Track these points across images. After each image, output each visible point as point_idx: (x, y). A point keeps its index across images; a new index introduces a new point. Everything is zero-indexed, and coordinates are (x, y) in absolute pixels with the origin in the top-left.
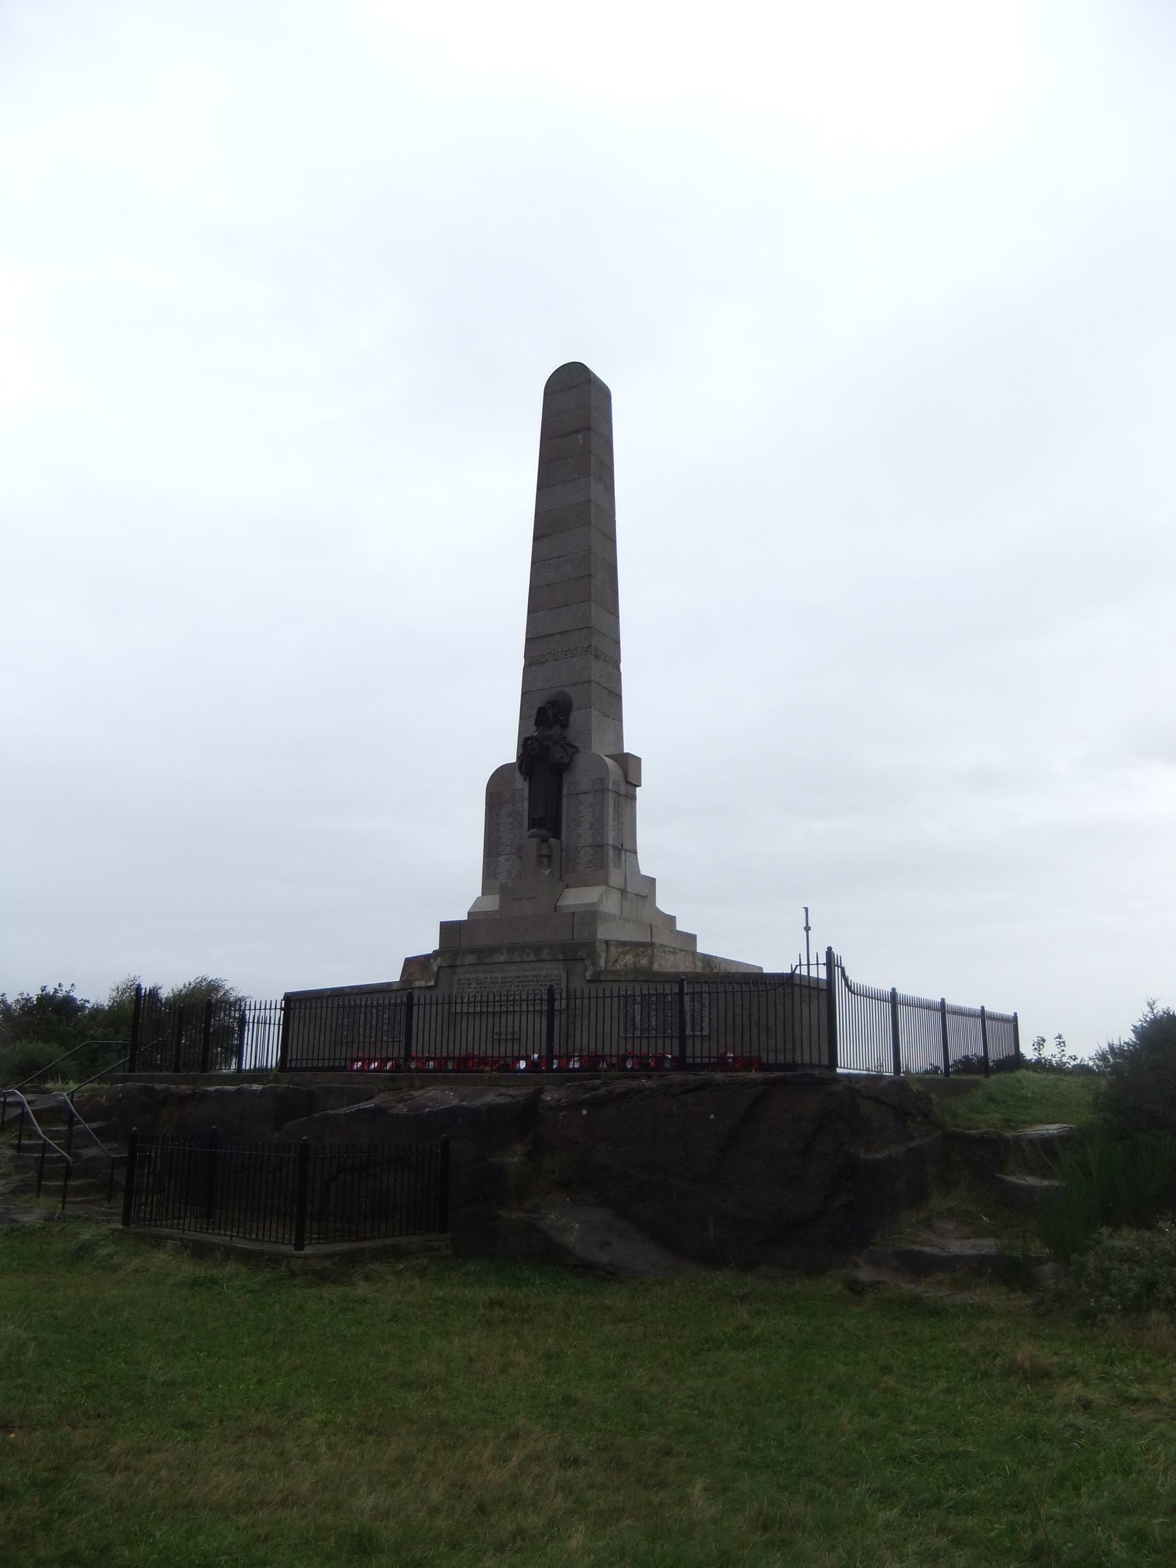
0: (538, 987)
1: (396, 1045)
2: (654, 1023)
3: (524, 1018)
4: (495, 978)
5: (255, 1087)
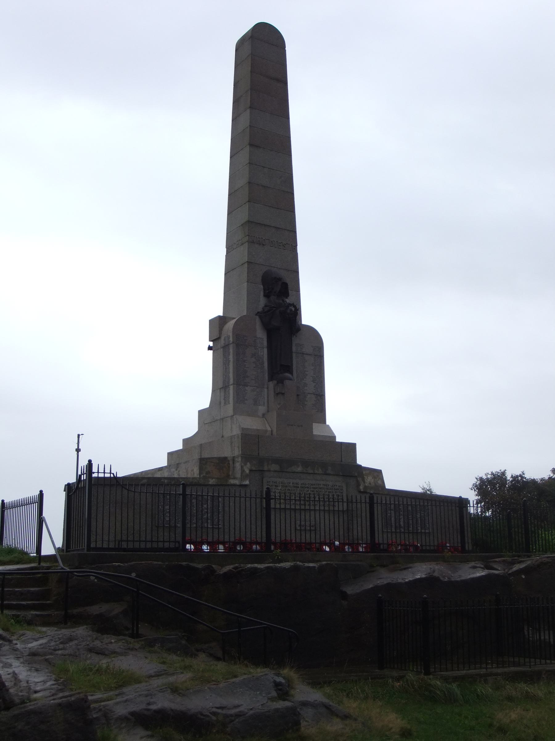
0: (327, 493)
1: (216, 531)
2: (402, 523)
3: (317, 515)
5: (311, 565)
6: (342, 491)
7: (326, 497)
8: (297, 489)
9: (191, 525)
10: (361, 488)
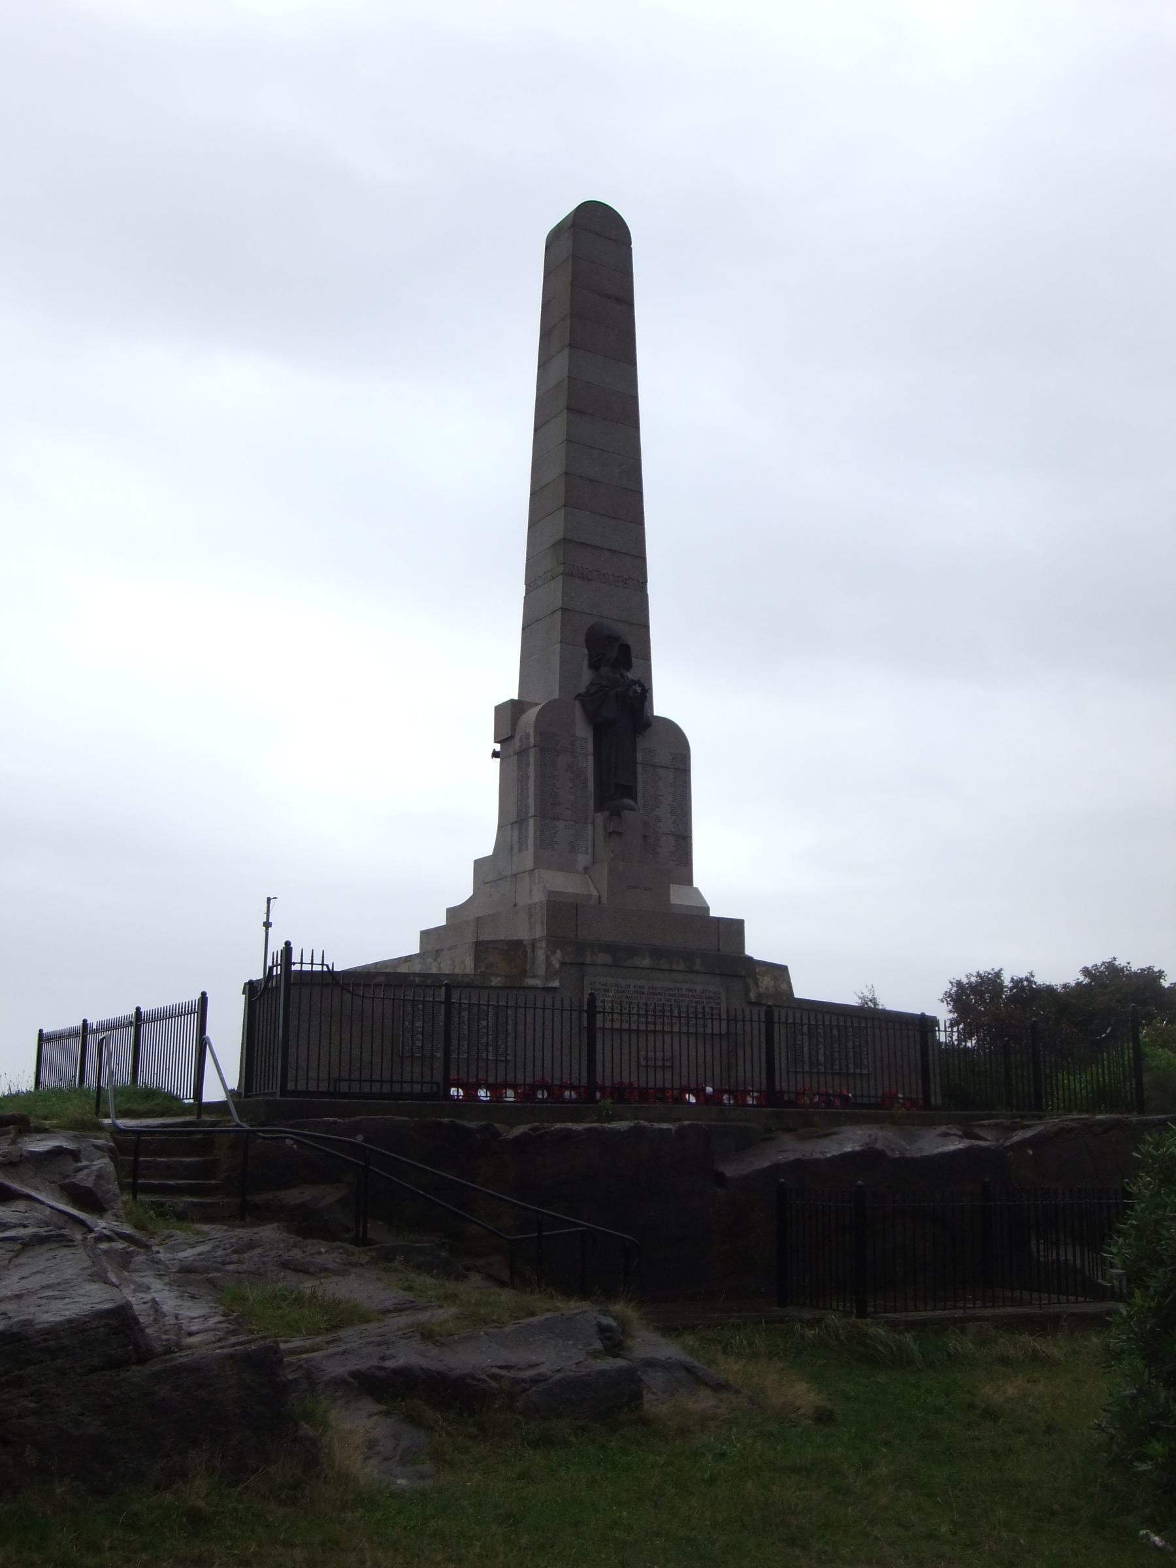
0: (694, 1005)
2: (821, 1058)
4: (641, 987)
5: (665, 1126)
6: (719, 1001)
7: (691, 1010)
8: (643, 995)
9: (458, 1055)
10: (752, 996)
